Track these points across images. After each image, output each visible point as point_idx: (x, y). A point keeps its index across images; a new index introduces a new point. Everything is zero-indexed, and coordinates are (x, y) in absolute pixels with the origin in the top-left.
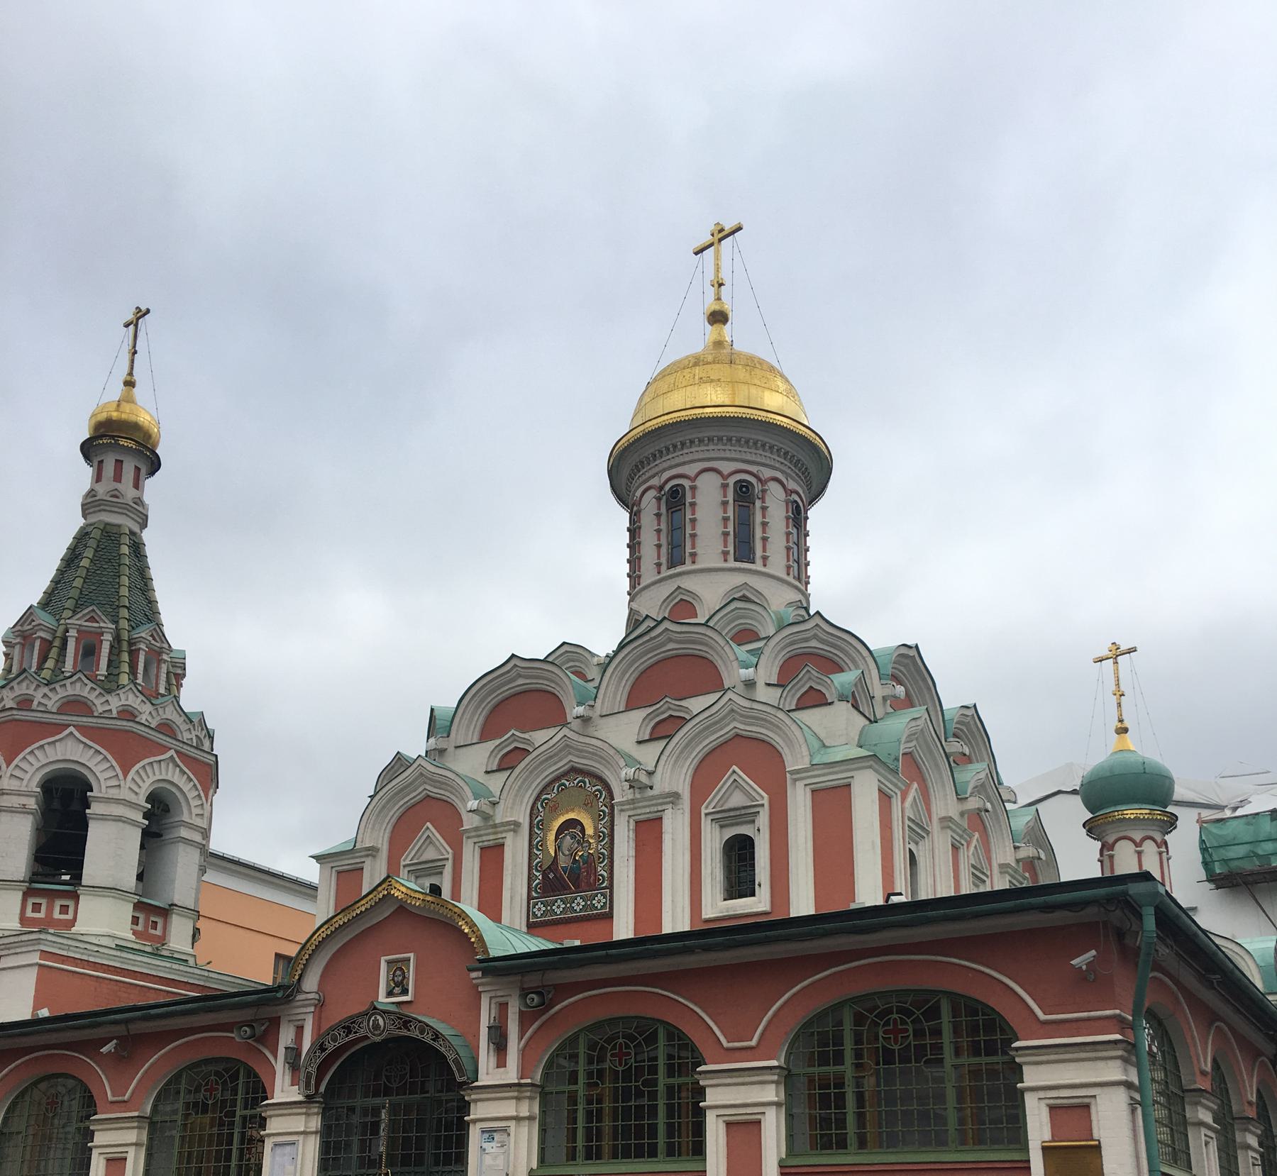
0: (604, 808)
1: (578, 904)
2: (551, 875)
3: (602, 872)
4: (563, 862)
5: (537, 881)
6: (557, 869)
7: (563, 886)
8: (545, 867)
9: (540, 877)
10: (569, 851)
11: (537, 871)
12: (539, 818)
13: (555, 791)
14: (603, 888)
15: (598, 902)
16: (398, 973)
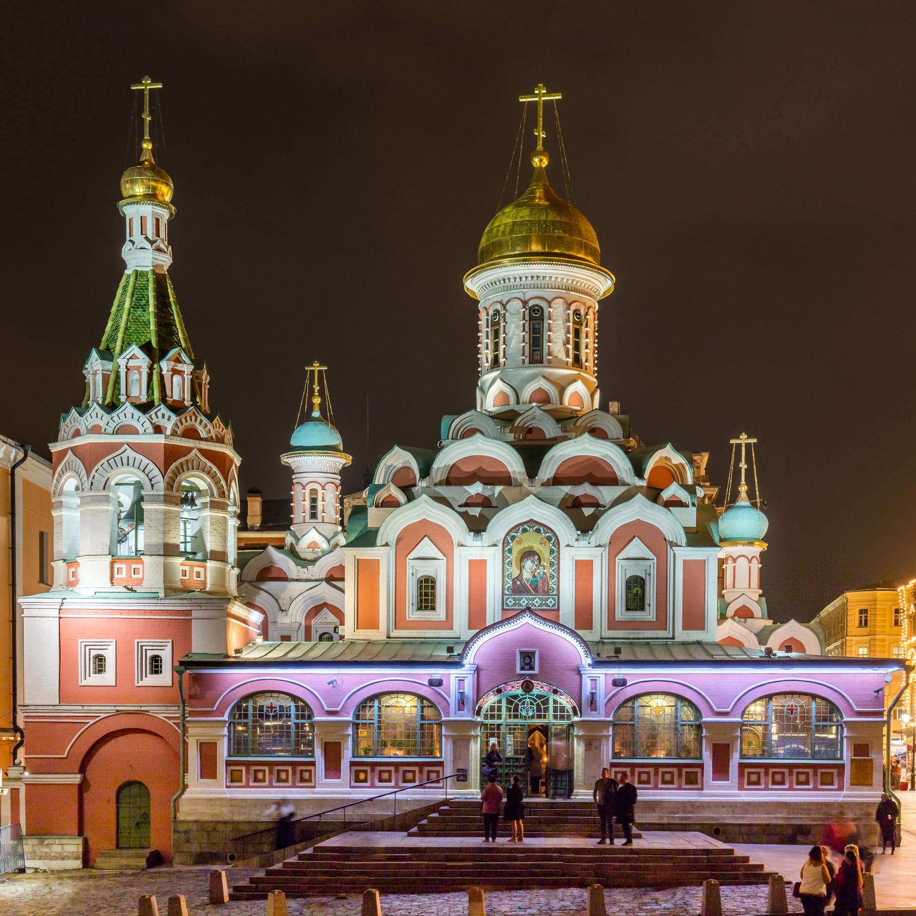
0: (553, 547)
1: (537, 602)
2: (518, 583)
3: (553, 585)
4: (527, 575)
5: (509, 585)
6: (521, 580)
7: (526, 589)
8: (513, 577)
9: (511, 583)
10: (530, 569)
11: (508, 578)
12: (509, 546)
13: (520, 532)
14: (553, 595)
15: (551, 602)
16: (527, 658)
